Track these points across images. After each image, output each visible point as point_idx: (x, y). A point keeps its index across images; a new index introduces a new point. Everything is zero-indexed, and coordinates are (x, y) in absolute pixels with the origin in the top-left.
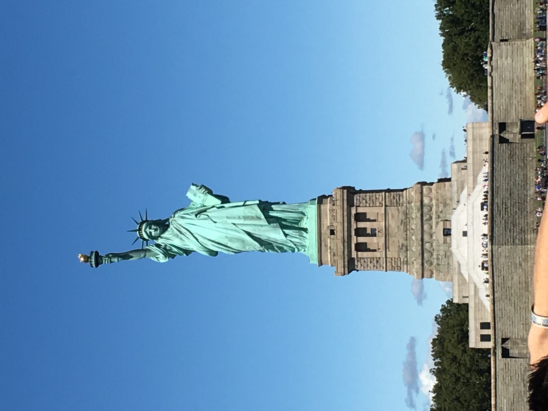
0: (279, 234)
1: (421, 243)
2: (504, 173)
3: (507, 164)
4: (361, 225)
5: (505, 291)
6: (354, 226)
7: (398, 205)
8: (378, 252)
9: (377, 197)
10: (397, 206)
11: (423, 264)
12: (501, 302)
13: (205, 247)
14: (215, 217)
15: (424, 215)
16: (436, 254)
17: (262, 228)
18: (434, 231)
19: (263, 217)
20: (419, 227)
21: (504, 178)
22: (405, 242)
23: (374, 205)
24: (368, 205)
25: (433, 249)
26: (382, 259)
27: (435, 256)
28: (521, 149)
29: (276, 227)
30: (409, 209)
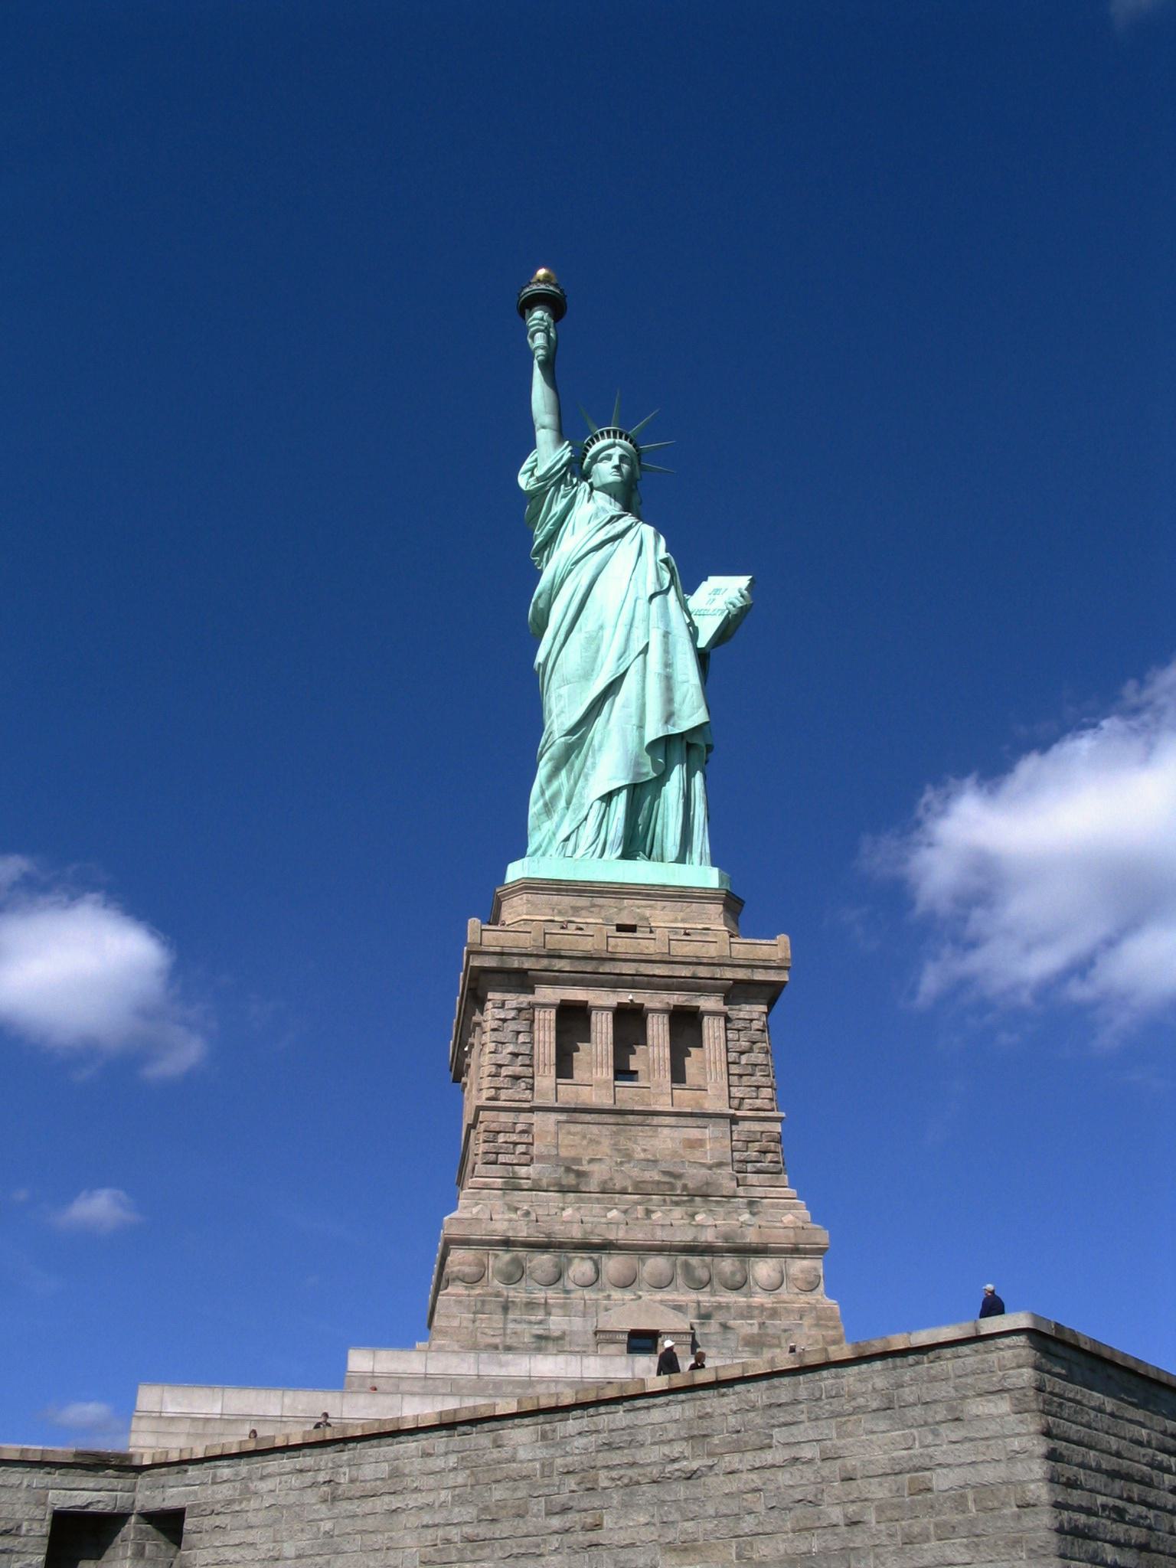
1: (596, 1240)
4: (658, 1028)
5: (562, 1498)
7: (737, 1166)
9: (766, 1092)
10: (733, 1161)
11: (507, 1243)
12: (461, 1478)
13: (570, 571)
14: (665, 606)
15: (708, 1259)
16: (549, 1301)
17: (635, 727)
18: (646, 1297)
20: (661, 1236)
22: (593, 1184)
23: (736, 1078)
26: (527, 1095)
27: (543, 1295)
29: (638, 774)
30: (729, 1202)
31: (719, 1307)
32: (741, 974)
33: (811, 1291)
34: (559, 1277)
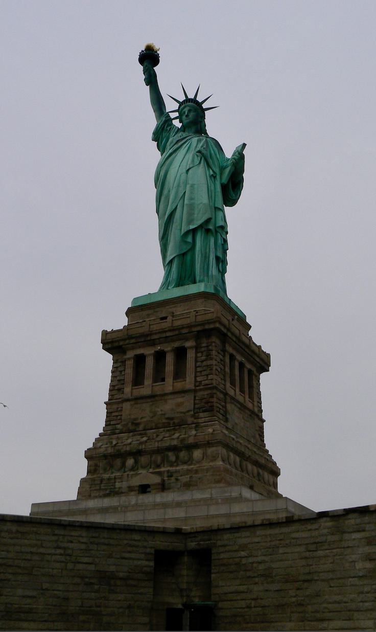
0: (171, 255)
2: (49, 557)
3: (81, 566)
4: (170, 359)
6: (168, 348)
8: (132, 389)
9: (210, 377)
11: (105, 456)
19: (192, 227)
21: (28, 557)
22: (141, 427)
23: (198, 374)
24: (198, 364)
25: (125, 472)
26: (121, 396)
28: (129, 607)
31: (176, 472)
32: (199, 328)
33: (215, 460)
34: (124, 465)
